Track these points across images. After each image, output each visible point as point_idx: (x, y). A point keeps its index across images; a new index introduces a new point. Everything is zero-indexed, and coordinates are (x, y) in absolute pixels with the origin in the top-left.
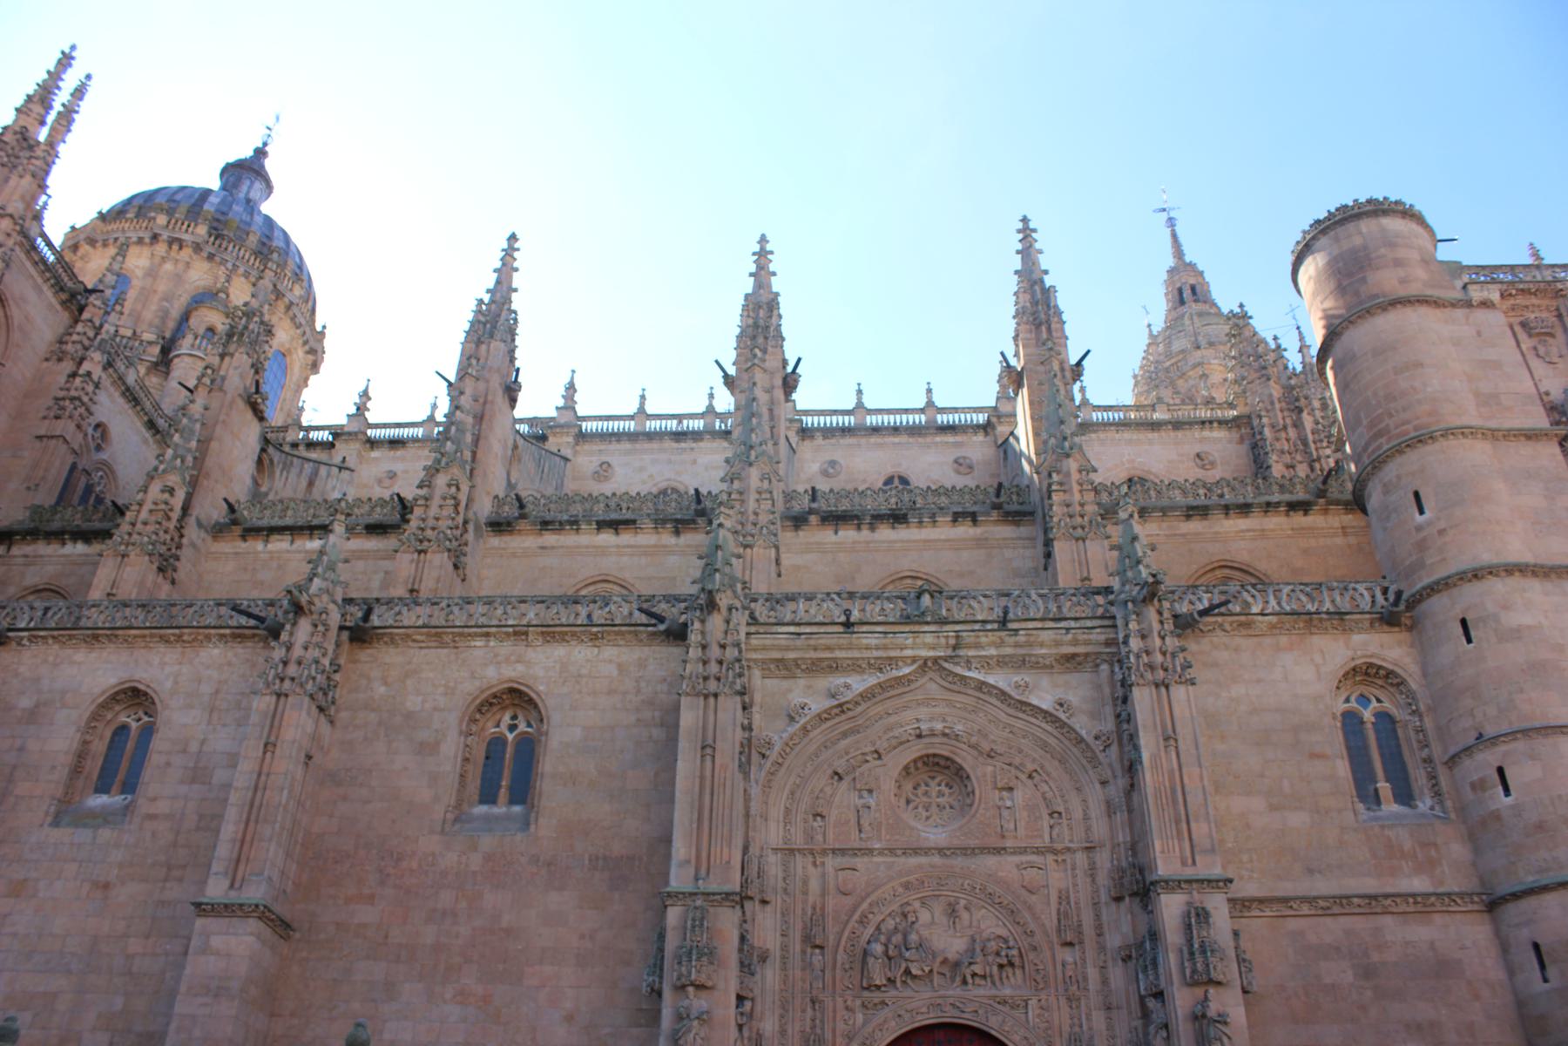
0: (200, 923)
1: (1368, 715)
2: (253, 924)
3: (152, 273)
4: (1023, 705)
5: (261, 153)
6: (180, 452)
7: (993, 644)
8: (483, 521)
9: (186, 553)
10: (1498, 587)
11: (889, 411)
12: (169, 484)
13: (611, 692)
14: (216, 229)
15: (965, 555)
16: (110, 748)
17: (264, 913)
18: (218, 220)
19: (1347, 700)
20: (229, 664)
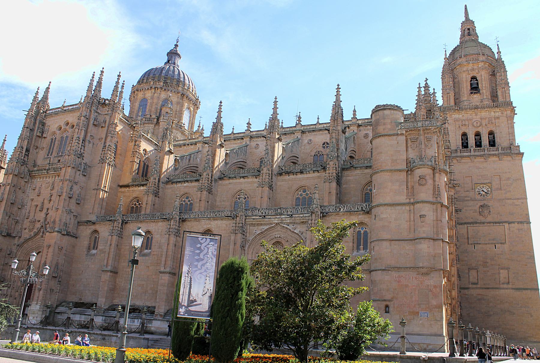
0: (160, 274)
1: (362, 232)
2: (168, 275)
3: (152, 98)
4: (293, 232)
5: (176, 46)
6: (156, 169)
7: (288, 220)
8: (217, 178)
9: (160, 190)
10: (382, 208)
11: (325, 123)
12: (154, 177)
13: (224, 230)
14: (165, 81)
15: (316, 180)
16: (147, 241)
17: (170, 273)
18: (166, 78)
19: (359, 229)
20: (163, 226)
